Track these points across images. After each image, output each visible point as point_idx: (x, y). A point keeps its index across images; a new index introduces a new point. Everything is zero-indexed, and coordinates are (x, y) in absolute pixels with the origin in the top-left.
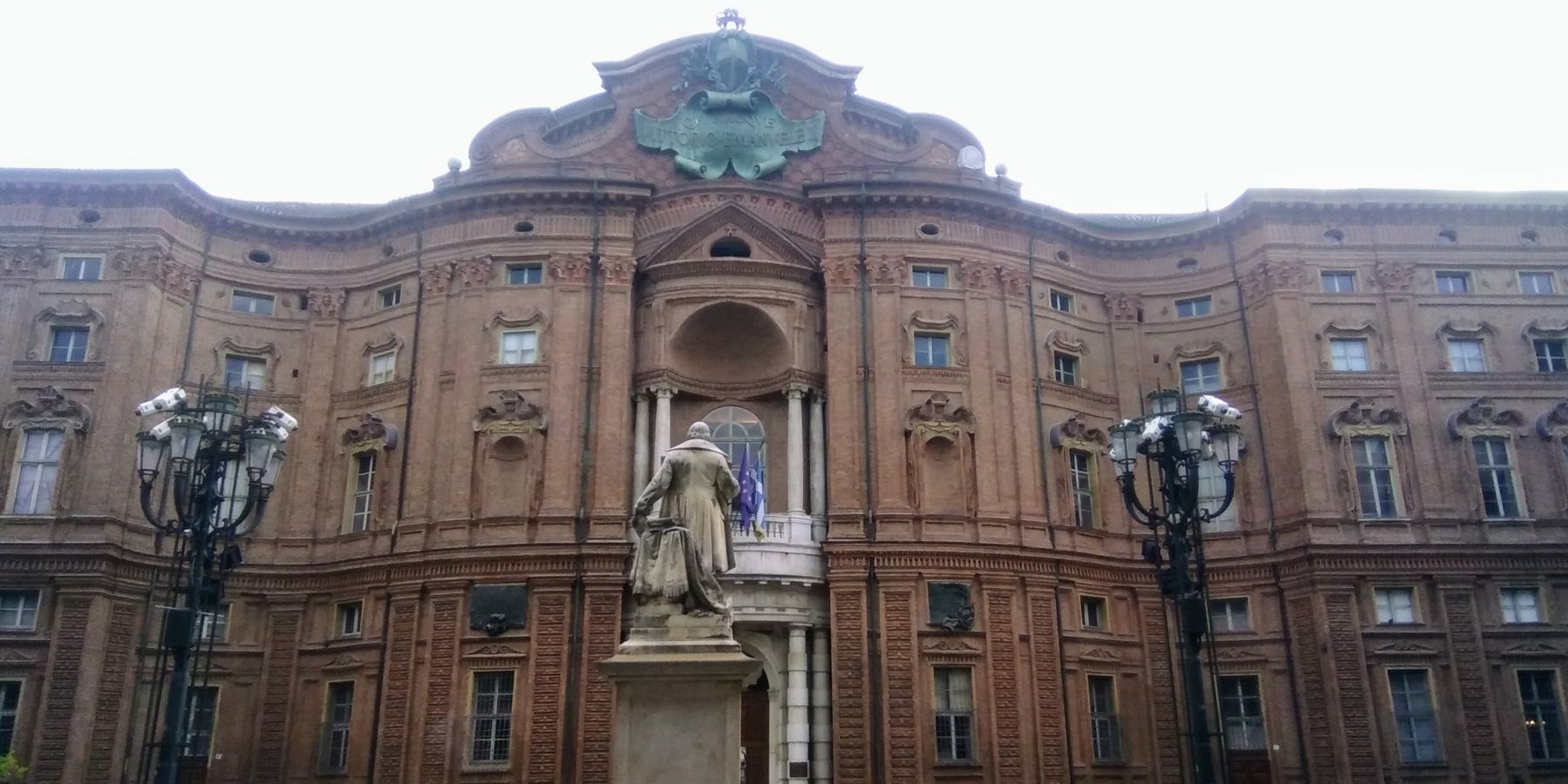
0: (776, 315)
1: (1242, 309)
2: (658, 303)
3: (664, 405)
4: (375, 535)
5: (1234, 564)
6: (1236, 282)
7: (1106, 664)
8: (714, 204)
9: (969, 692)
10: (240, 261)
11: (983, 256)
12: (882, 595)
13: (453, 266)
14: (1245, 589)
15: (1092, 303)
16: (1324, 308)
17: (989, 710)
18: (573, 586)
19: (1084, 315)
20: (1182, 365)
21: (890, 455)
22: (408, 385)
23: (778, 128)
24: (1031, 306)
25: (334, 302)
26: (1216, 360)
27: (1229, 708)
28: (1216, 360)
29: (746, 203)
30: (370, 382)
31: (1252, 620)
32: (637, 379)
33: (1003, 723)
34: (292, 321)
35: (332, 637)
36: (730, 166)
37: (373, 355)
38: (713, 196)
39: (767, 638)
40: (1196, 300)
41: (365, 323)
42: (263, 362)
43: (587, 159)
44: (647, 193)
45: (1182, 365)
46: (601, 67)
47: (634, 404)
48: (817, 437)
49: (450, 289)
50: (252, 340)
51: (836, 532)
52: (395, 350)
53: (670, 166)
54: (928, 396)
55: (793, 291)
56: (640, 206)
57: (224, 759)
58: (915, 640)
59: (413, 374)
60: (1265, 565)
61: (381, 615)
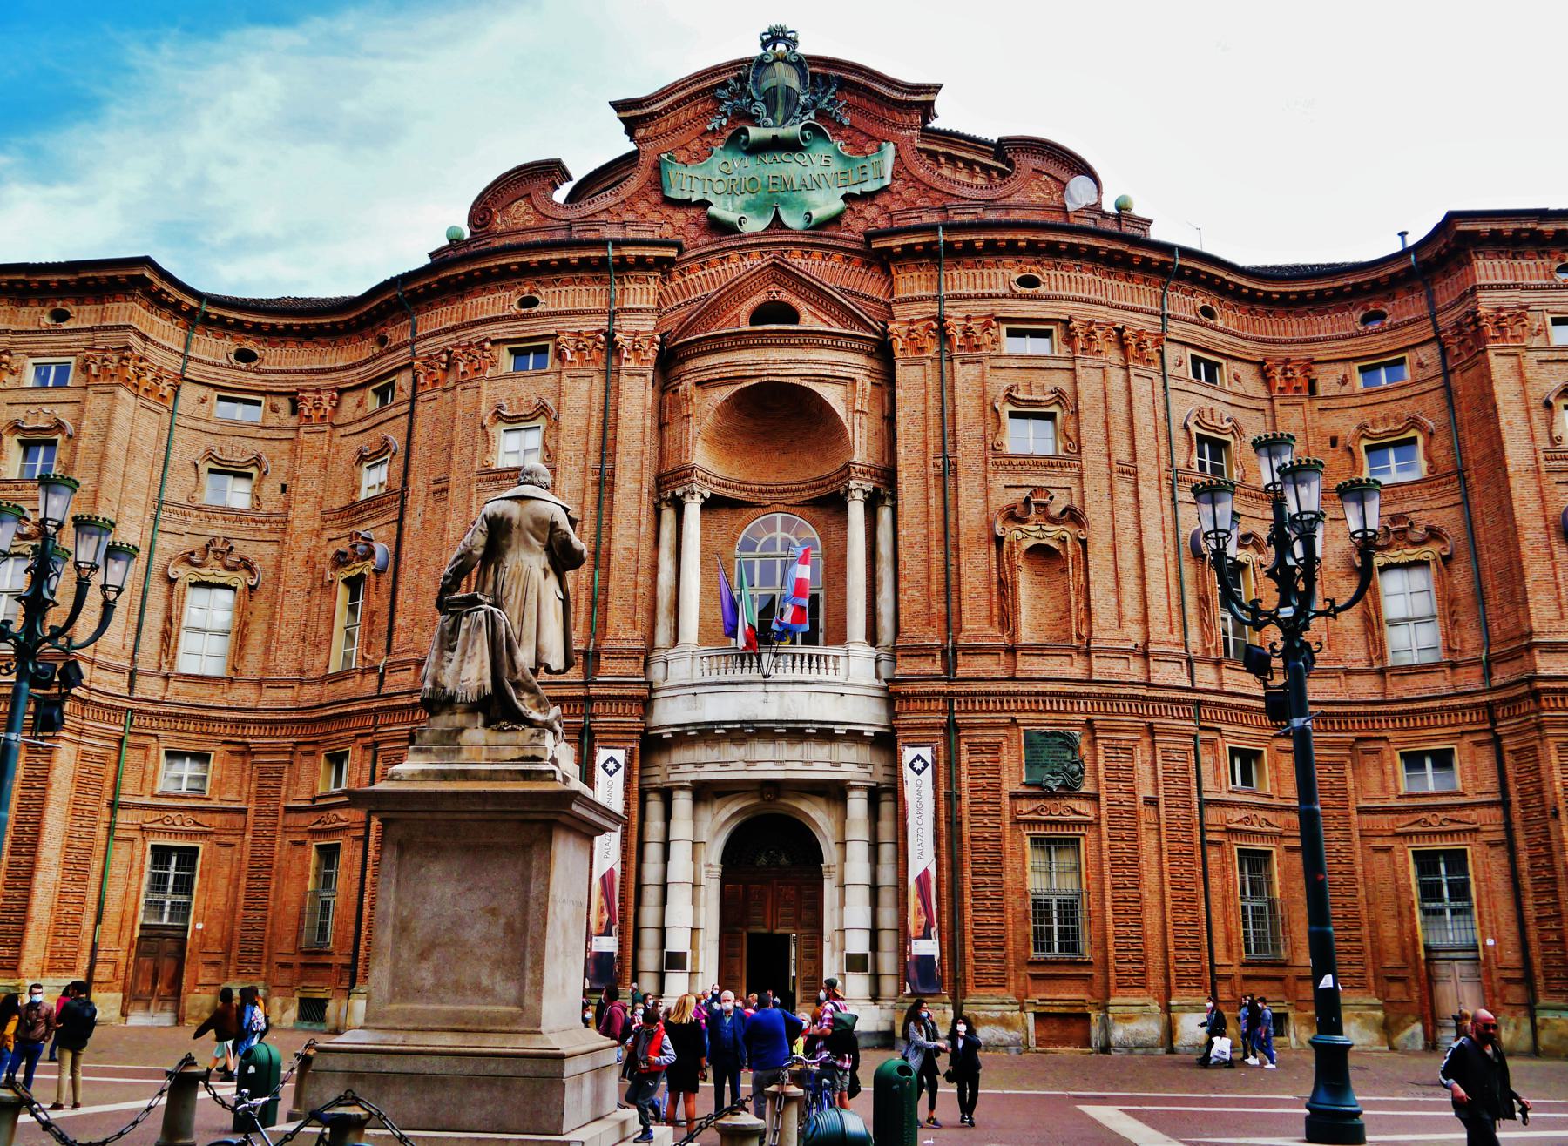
0: (832, 395)
1: (1446, 373)
2: (687, 385)
3: (693, 510)
4: (363, 673)
5: (1437, 704)
6: (1437, 338)
8: (756, 261)
9: (1077, 869)
10: (224, 361)
11: (1101, 314)
12: (964, 747)
13: (449, 353)
14: (1451, 737)
15: (1248, 373)
16: (1555, 367)
17: (1103, 892)
18: (581, 735)
19: (1237, 387)
20: (1368, 449)
21: (975, 569)
22: (397, 496)
23: (836, 166)
24: (1164, 376)
25: (326, 404)
26: (1413, 441)
27: (1430, 891)
28: (1413, 441)
29: (797, 261)
30: (363, 495)
31: (1458, 778)
32: (663, 481)
33: (1123, 907)
34: (280, 428)
35: (320, 792)
36: (777, 217)
37: (366, 465)
38: (755, 252)
39: (821, 802)
40: (1387, 365)
41: (358, 427)
42: (249, 476)
43: (603, 217)
44: (673, 253)
45: (1368, 449)
46: (619, 106)
47: (658, 514)
48: (885, 549)
49: (444, 380)
50: (237, 450)
51: (907, 666)
52: (388, 457)
53: (703, 219)
54: (1027, 492)
55: (855, 364)
56: (664, 266)
57: (206, 929)
58: (1006, 804)
59: (405, 483)
60: (1477, 706)
61: (368, 767)
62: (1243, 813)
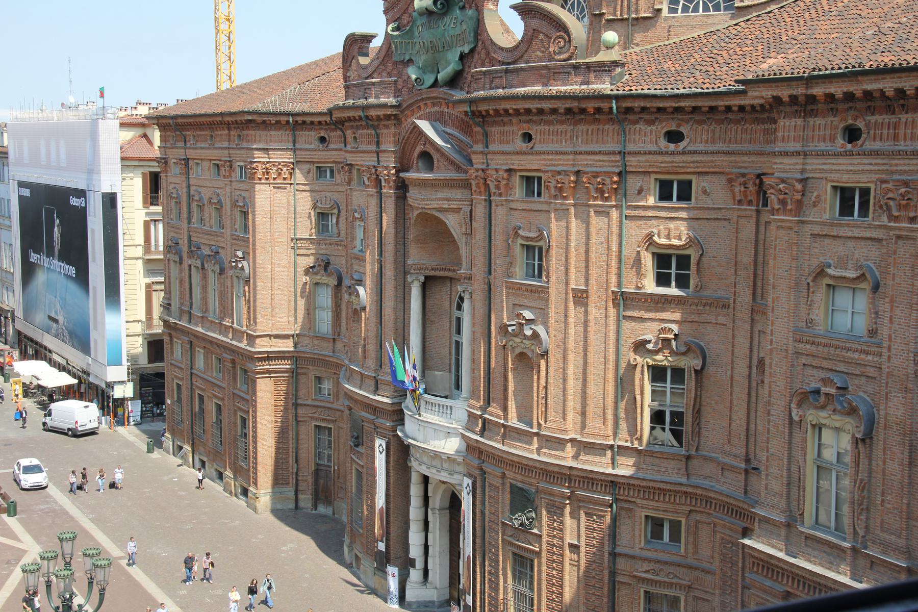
0: (453, 222)
7: (670, 585)
16: (827, 241)
62: (646, 566)
